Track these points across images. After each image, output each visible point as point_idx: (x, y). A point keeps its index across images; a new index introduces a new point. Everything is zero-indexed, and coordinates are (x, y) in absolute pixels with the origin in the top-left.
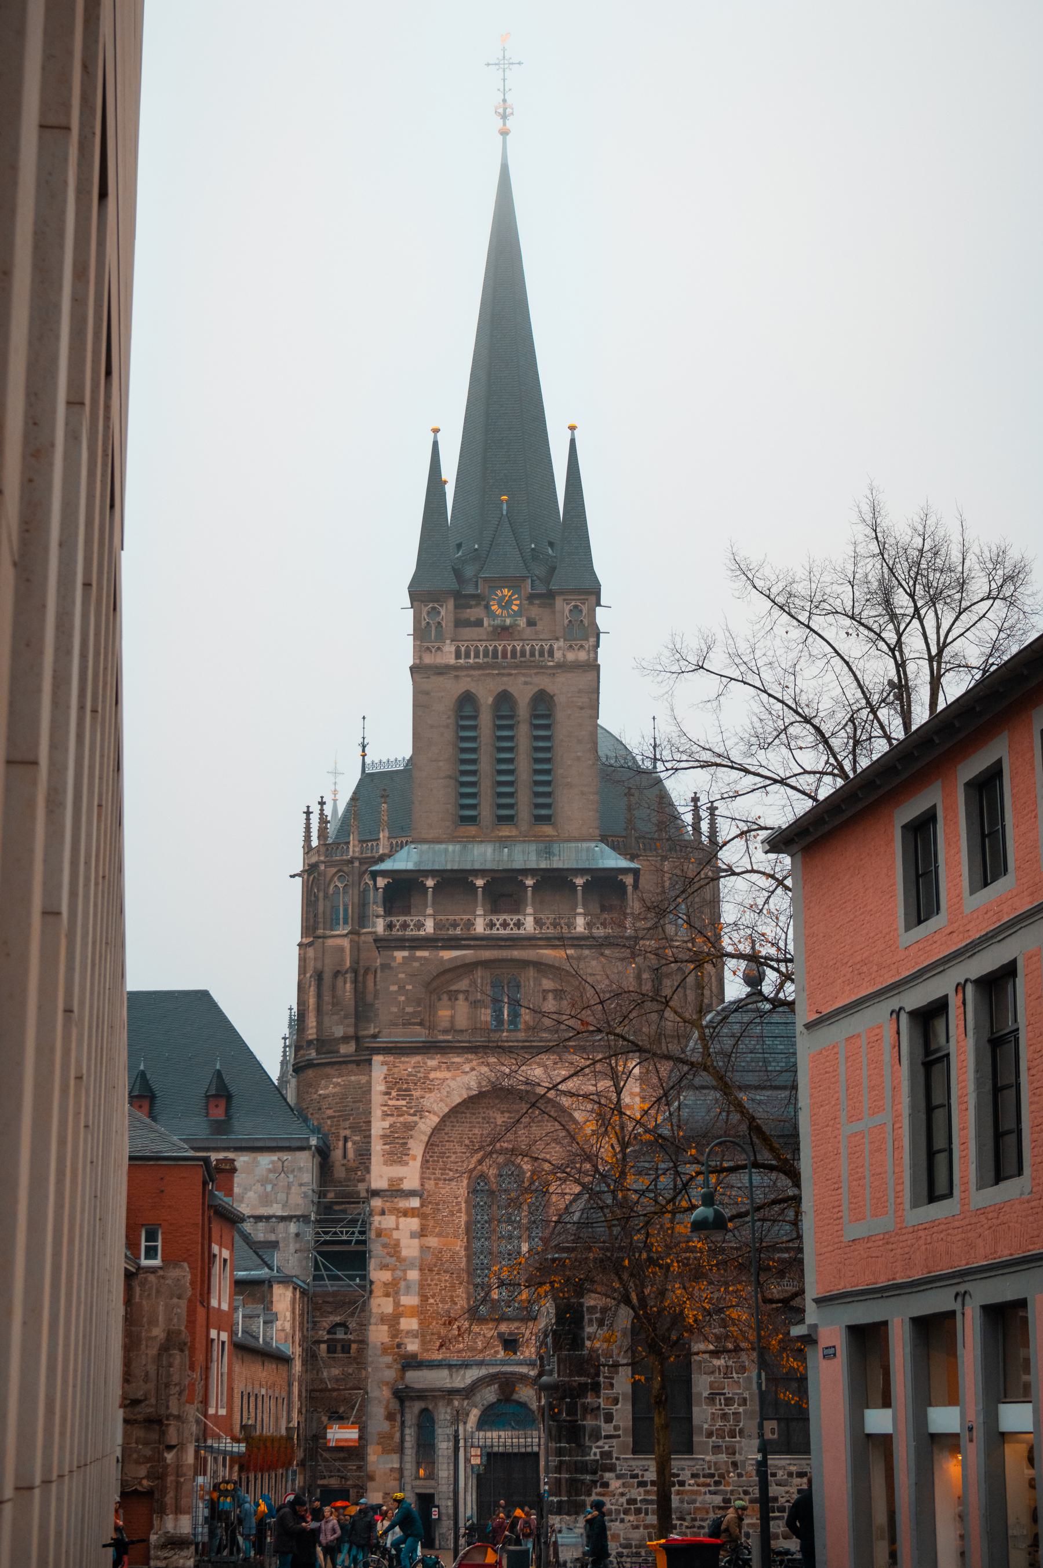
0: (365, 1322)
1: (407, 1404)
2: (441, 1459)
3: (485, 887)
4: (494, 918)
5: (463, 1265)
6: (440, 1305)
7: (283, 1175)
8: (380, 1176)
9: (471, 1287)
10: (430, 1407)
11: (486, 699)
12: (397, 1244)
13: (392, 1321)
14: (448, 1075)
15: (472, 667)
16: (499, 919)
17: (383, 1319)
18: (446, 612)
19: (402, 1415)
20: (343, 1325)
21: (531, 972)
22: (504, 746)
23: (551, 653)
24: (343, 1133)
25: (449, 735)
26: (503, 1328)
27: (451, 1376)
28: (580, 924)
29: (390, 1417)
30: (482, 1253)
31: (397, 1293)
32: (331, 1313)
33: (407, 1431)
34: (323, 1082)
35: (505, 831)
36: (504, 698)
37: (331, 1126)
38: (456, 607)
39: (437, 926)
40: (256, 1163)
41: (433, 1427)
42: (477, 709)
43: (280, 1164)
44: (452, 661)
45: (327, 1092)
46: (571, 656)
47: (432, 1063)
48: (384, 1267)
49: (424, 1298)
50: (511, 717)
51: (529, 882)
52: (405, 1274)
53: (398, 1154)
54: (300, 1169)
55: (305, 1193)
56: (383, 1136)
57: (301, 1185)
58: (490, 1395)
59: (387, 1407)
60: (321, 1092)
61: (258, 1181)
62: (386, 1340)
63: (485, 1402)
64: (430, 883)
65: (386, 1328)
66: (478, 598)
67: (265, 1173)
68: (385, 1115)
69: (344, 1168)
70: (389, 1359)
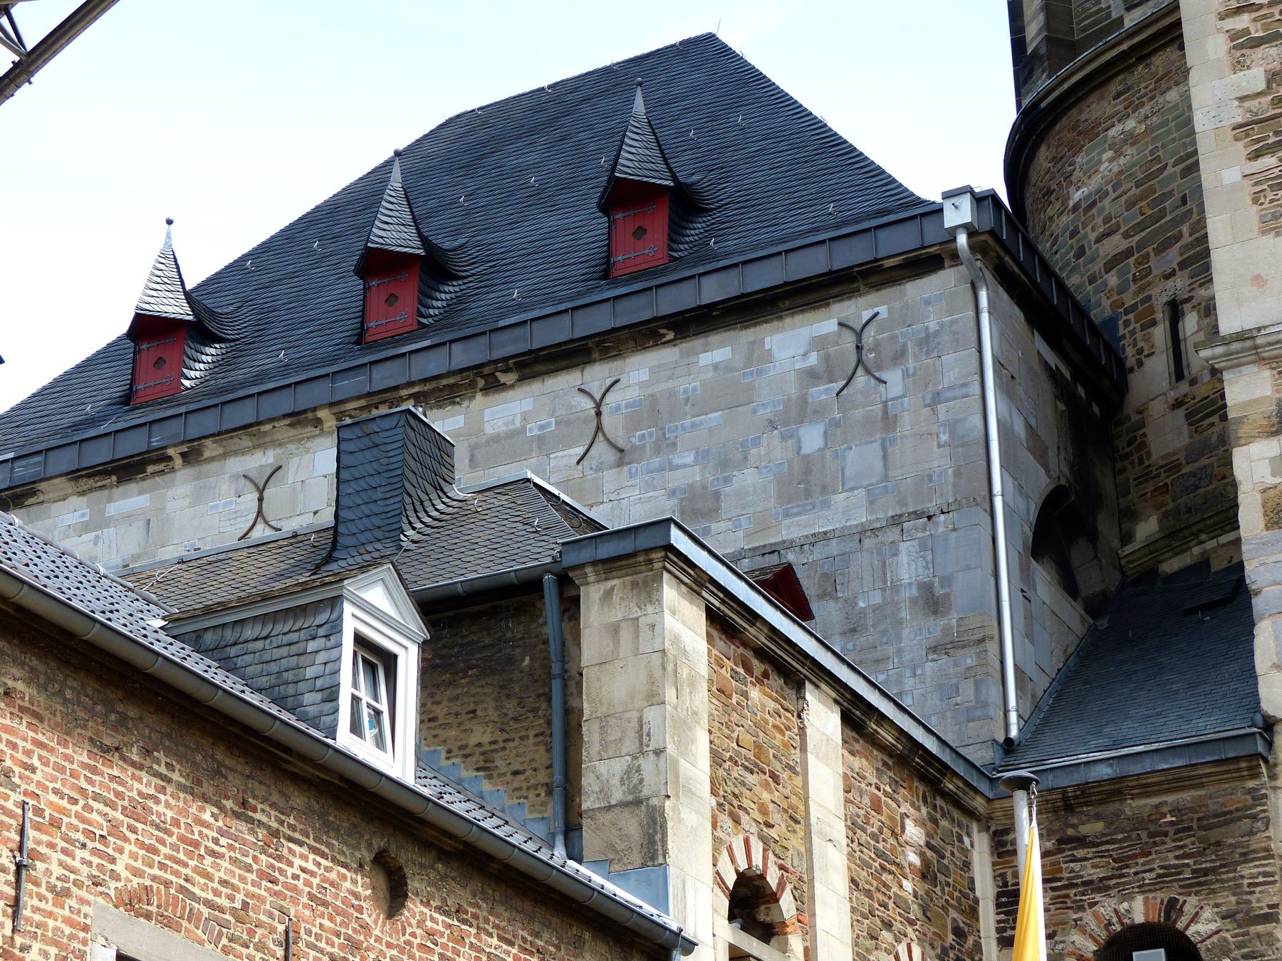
0: (1261, 901)
7: (861, 379)
24: (1161, 294)
32: (1101, 886)
34: (1078, 160)
37: (1122, 289)
40: (758, 358)
43: (849, 341)
45: (1095, 183)
54: (927, 342)
55: (953, 426)
56: (1242, 129)
57: (936, 399)
60: (1077, 196)
61: (772, 425)
67: (793, 390)
68: (1243, 44)
69: (1181, 412)
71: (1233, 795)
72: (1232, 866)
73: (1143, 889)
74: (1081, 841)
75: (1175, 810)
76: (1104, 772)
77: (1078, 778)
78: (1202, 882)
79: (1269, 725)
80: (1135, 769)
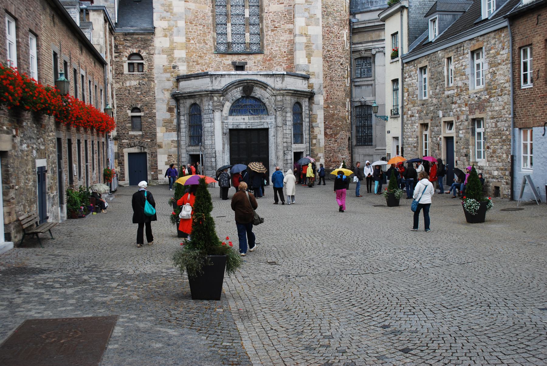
0: (152, 52)
1: (181, 101)
2: (206, 134)
5: (210, 21)
6: (197, 45)
9: (215, 34)
10: (198, 102)
12: (170, 5)
13: (169, 52)
17: (163, 51)
19: (178, 109)
20: (138, 54)
26: (236, 58)
27: (212, 82)
29: (170, 110)
30: (220, 15)
31: (171, 35)
32: (130, 47)
33: (182, 118)
41: (200, 115)
48: (163, 18)
49: (188, 40)
52: (176, 23)
58: (237, 93)
59: (168, 104)
62: (166, 63)
63: (234, 98)
65: (166, 56)
70: (168, 75)
71: (149, 37)
72: (148, 47)
73: (136, 48)
74: (127, 40)
75: (141, 38)
76: (132, 31)
77: (128, 31)
78: (144, 48)
79: (155, 28)
80: (136, 32)
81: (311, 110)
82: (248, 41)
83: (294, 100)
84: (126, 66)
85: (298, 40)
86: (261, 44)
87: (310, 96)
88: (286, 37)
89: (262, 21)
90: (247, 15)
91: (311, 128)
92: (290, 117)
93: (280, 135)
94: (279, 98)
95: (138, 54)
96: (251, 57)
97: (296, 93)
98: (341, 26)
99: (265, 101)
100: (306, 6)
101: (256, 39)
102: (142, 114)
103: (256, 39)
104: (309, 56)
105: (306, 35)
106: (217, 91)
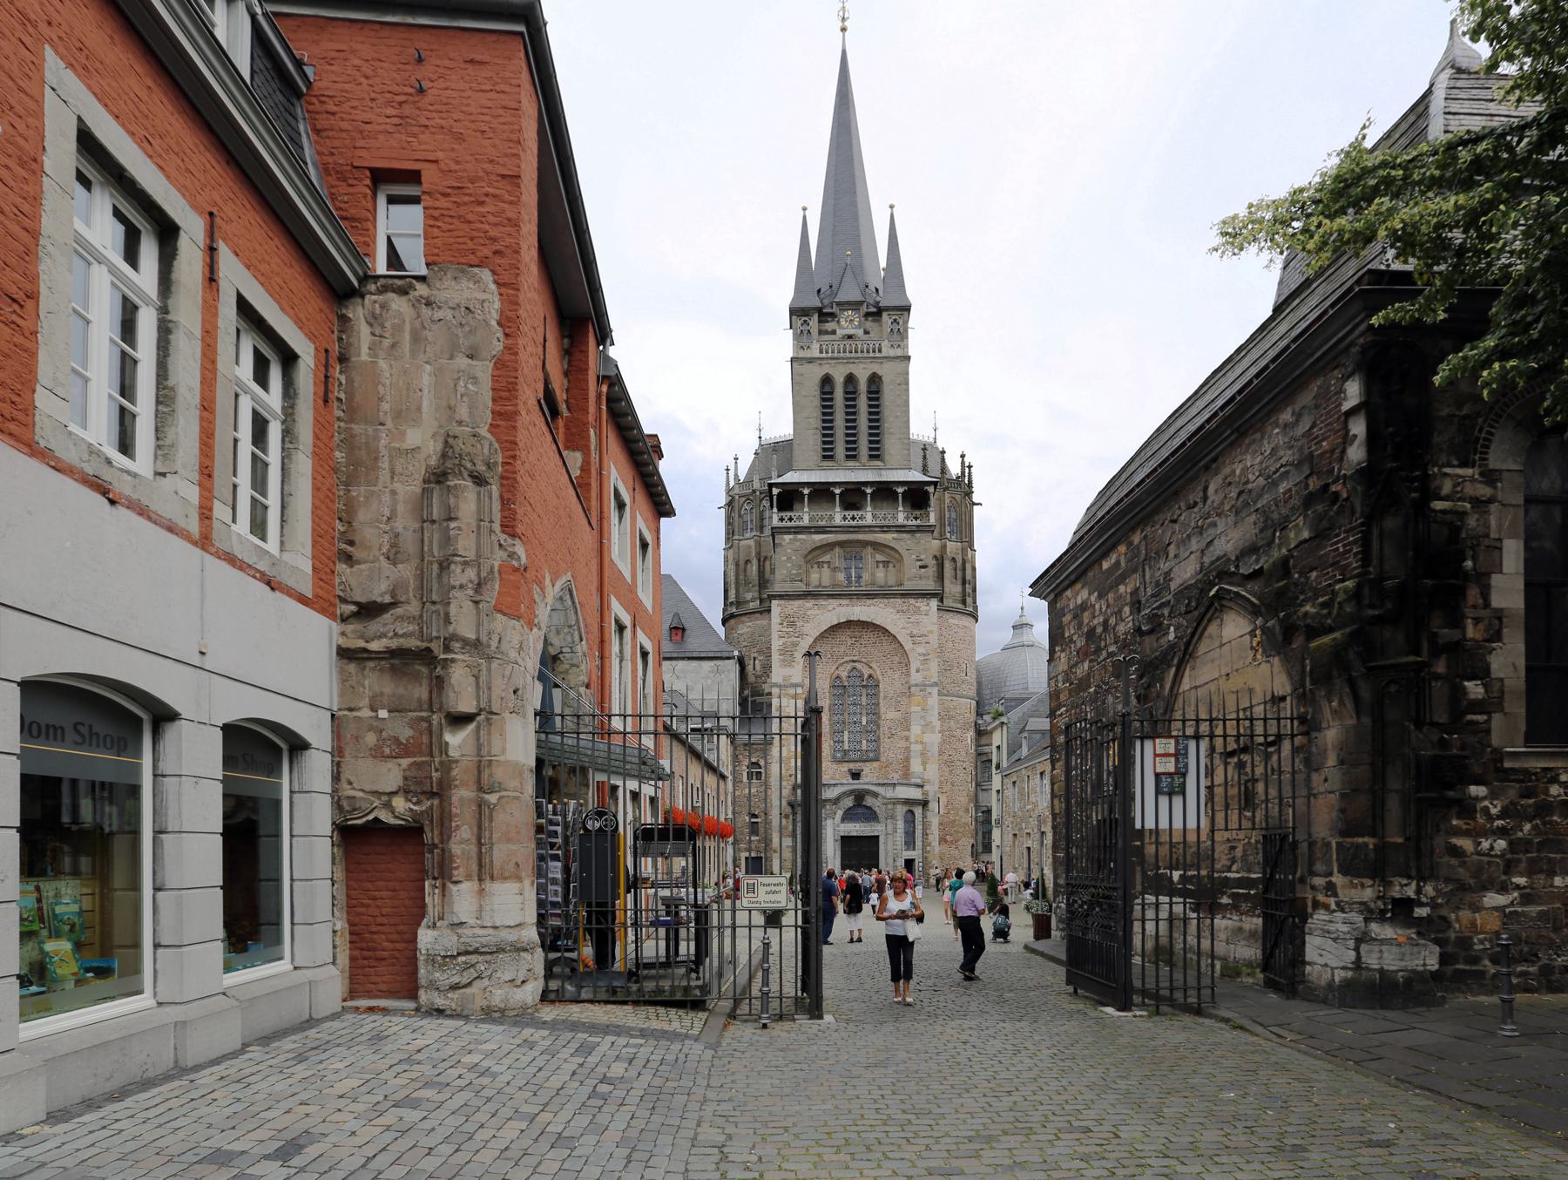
3: (841, 494)
4: (847, 513)
8: (778, 674)
11: (839, 380)
14: (819, 612)
15: (832, 358)
16: (849, 514)
18: (814, 321)
21: (869, 549)
22: (851, 411)
23: (880, 351)
25: (817, 402)
28: (901, 518)
35: (851, 464)
36: (850, 379)
38: (820, 322)
39: (811, 520)
42: (833, 387)
44: (816, 354)
46: (892, 353)
47: (809, 603)
50: (854, 393)
51: (869, 491)
53: (788, 660)
58: (849, 802)
64: (806, 491)
66: (833, 315)
81: (924, 817)
82: (864, 748)
83: (905, 808)
84: (745, 774)
85: (913, 747)
86: (877, 751)
87: (925, 804)
88: (902, 744)
89: (879, 728)
90: (864, 723)
91: (925, 834)
92: (901, 825)
93: (890, 843)
94: (890, 807)
95: (757, 764)
96: (868, 764)
97: (907, 802)
98: (965, 729)
99: (876, 809)
100: (922, 714)
101: (872, 746)
102: (759, 820)
103: (872, 746)
104: (924, 763)
105: (922, 743)
106: (829, 800)
